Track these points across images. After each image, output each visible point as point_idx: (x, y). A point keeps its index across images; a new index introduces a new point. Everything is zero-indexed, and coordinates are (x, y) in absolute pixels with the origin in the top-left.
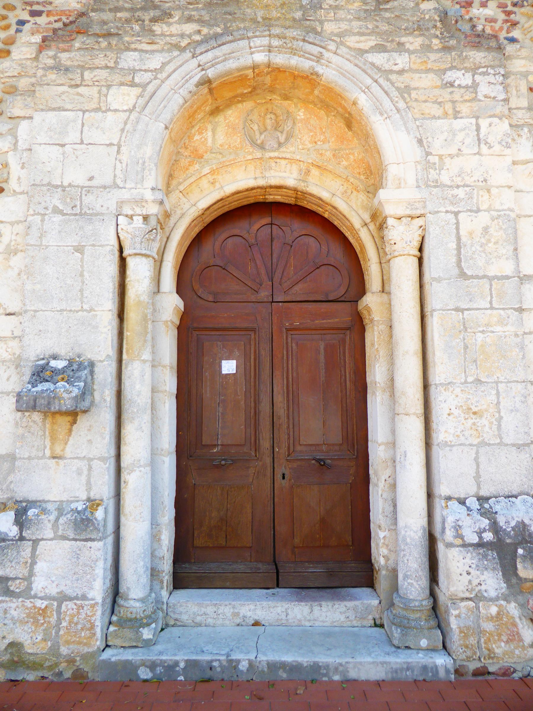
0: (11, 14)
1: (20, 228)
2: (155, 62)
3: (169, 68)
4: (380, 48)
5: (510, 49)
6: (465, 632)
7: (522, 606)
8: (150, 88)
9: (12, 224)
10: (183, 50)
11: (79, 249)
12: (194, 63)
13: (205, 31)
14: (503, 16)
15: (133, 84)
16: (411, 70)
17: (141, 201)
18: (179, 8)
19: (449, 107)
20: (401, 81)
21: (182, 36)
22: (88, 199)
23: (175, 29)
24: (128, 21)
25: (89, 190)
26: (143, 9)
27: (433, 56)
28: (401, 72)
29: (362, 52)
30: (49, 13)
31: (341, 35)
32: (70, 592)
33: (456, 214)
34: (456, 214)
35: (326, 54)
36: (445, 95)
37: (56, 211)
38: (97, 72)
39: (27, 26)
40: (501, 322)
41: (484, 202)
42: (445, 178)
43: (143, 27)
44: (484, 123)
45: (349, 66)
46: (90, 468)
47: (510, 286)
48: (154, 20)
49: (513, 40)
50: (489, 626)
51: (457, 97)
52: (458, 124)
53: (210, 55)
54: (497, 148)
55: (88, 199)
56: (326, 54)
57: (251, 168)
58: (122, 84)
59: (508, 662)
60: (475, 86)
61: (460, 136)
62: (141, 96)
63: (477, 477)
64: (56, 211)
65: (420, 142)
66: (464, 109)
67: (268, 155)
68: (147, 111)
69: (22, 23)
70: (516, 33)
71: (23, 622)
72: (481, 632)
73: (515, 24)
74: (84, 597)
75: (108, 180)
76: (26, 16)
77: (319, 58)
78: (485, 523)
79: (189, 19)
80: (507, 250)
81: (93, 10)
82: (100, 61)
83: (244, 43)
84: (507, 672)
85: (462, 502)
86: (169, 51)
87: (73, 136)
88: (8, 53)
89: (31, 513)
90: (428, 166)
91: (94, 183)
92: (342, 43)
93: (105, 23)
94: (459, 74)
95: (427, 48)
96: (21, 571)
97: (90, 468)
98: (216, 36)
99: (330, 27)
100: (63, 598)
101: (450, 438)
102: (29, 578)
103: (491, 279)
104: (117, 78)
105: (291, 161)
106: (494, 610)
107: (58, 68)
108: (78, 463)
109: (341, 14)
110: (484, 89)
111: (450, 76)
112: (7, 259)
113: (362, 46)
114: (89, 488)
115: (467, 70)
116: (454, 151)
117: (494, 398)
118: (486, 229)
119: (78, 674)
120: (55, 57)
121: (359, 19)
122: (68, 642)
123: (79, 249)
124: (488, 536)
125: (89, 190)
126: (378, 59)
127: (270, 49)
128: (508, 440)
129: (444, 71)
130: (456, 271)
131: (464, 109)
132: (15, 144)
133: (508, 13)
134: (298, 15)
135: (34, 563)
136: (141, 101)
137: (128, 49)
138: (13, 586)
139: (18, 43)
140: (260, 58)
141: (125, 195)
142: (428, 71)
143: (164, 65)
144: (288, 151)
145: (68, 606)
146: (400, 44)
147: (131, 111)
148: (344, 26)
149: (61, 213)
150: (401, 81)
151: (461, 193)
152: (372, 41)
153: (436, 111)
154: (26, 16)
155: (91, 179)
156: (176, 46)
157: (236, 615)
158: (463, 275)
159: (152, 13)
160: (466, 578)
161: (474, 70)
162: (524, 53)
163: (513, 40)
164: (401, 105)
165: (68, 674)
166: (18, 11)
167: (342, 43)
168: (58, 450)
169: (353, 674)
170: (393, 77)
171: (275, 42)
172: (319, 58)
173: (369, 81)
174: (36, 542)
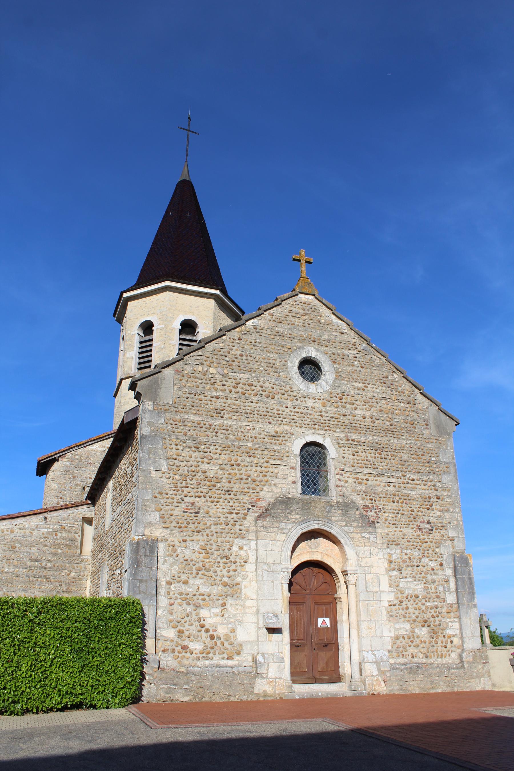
0: (245, 505)
1: (254, 574)
2: (289, 526)
3: (293, 529)
4: (346, 526)
5: (377, 525)
6: (369, 684)
7: (382, 677)
8: (288, 535)
9: (251, 572)
10: (296, 523)
11: (273, 582)
12: (299, 527)
13: (302, 518)
14: (375, 515)
15: (284, 533)
16: (354, 532)
17: (288, 568)
18: (295, 510)
19: (363, 543)
20: (352, 535)
21: (296, 519)
22: (274, 567)
23: (294, 517)
24: (281, 513)
25: (274, 564)
26: (285, 509)
27: (359, 529)
28: (351, 533)
29: (342, 526)
30: (257, 507)
31: (336, 521)
32: (278, 677)
33: (365, 574)
34: (365, 574)
35: (333, 527)
36: (362, 540)
37: (266, 570)
38: (274, 529)
39: (251, 510)
40: (376, 604)
41: (372, 570)
42: (363, 564)
43: (285, 515)
44: (372, 549)
45: (339, 531)
46: (278, 644)
47: (378, 594)
48: (288, 513)
49: (378, 522)
50: (374, 683)
51: (365, 541)
52: (366, 549)
53: (304, 525)
54: (375, 556)
55: (274, 567)
56: (333, 527)
57: (308, 554)
58: (281, 533)
59: (379, 691)
60: (370, 537)
61: (366, 552)
62: (286, 537)
63: (371, 645)
64: (266, 570)
65: (356, 553)
66: (367, 544)
67: (313, 550)
68: (288, 541)
69: (249, 509)
70: (379, 521)
71: (266, 685)
72: (373, 684)
73: (379, 518)
74: (281, 678)
75: (279, 562)
76: (250, 507)
77: (331, 528)
78: (374, 657)
79: (298, 514)
80: (377, 585)
81: (271, 509)
82: (275, 525)
83: (312, 522)
84: (379, 694)
85: (368, 652)
86: (293, 523)
87: (269, 548)
88: (246, 518)
89: (266, 656)
90: (358, 560)
91: (275, 562)
92: (337, 524)
93: (275, 513)
94: (366, 534)
95: (358, 526)
96: (265, 671)
97: (278, 644)
98: (305, 520)
99: (333, 519)
100: (276, 678)
101: (365, 635)
102: (267, 673)
103: (374, 592)
104: (280, 531)
105: (319, 552)
106: (376, 678)
107: (262, 526)
108: (275, 643)
109: (336, 515)
110: (372, 539)
111: (364, 534)
112: (250, 583)
113: (341, 524)
114: (278, 650)
115: (367, 533)
116: (364, 556)
117: (374, 624)
118: (372, 579)
119: (281, 698)
120: (262, 523)
121: (341, 516)
122: (278, 690)
123: (273, 582)
124: (374, 660)
125: (274, 564)
126: (346, 529)
127: (319, 524)
128: (378, 636)
129: (362, 533)
130: (365, 590)
131: (367, 544)
132: (250, 547)
133: (377, 514)
134: (326, 514)
135: (268, 669)
136: (286, 538)
137: (282, 522)
138: (264, 675)
139: (248, 516)
140: (316, 527)
141: (284, 567)
142: (358, 533)
143: (292, 527)
144: (318, 549)
145: (277, 680)
146: (351, 525)
147: (284, 541)
148: (337, 518)
149: (267, 571)
150: (352, 535)
151: (366, 568)
152: (343, 524)
153: (360, 545)
154: (250, 507)
155: (274, 561)
156: (294, 522)
157: (309, 688)
158: (367, 591)
159: (288, 511)
160: (369, 671)
161: (369, 533)
162: (381, 527)
163: (378, 522)
164: (352, 543)
165: (278, 698)
166: (247, 504)
167: (337, 524)
168: (270, 639)
169: (345, 695)
170: (349, 534)
171: (320, 522)
172: (331, 528)
173: (344, 535)
174: (268, 664)
